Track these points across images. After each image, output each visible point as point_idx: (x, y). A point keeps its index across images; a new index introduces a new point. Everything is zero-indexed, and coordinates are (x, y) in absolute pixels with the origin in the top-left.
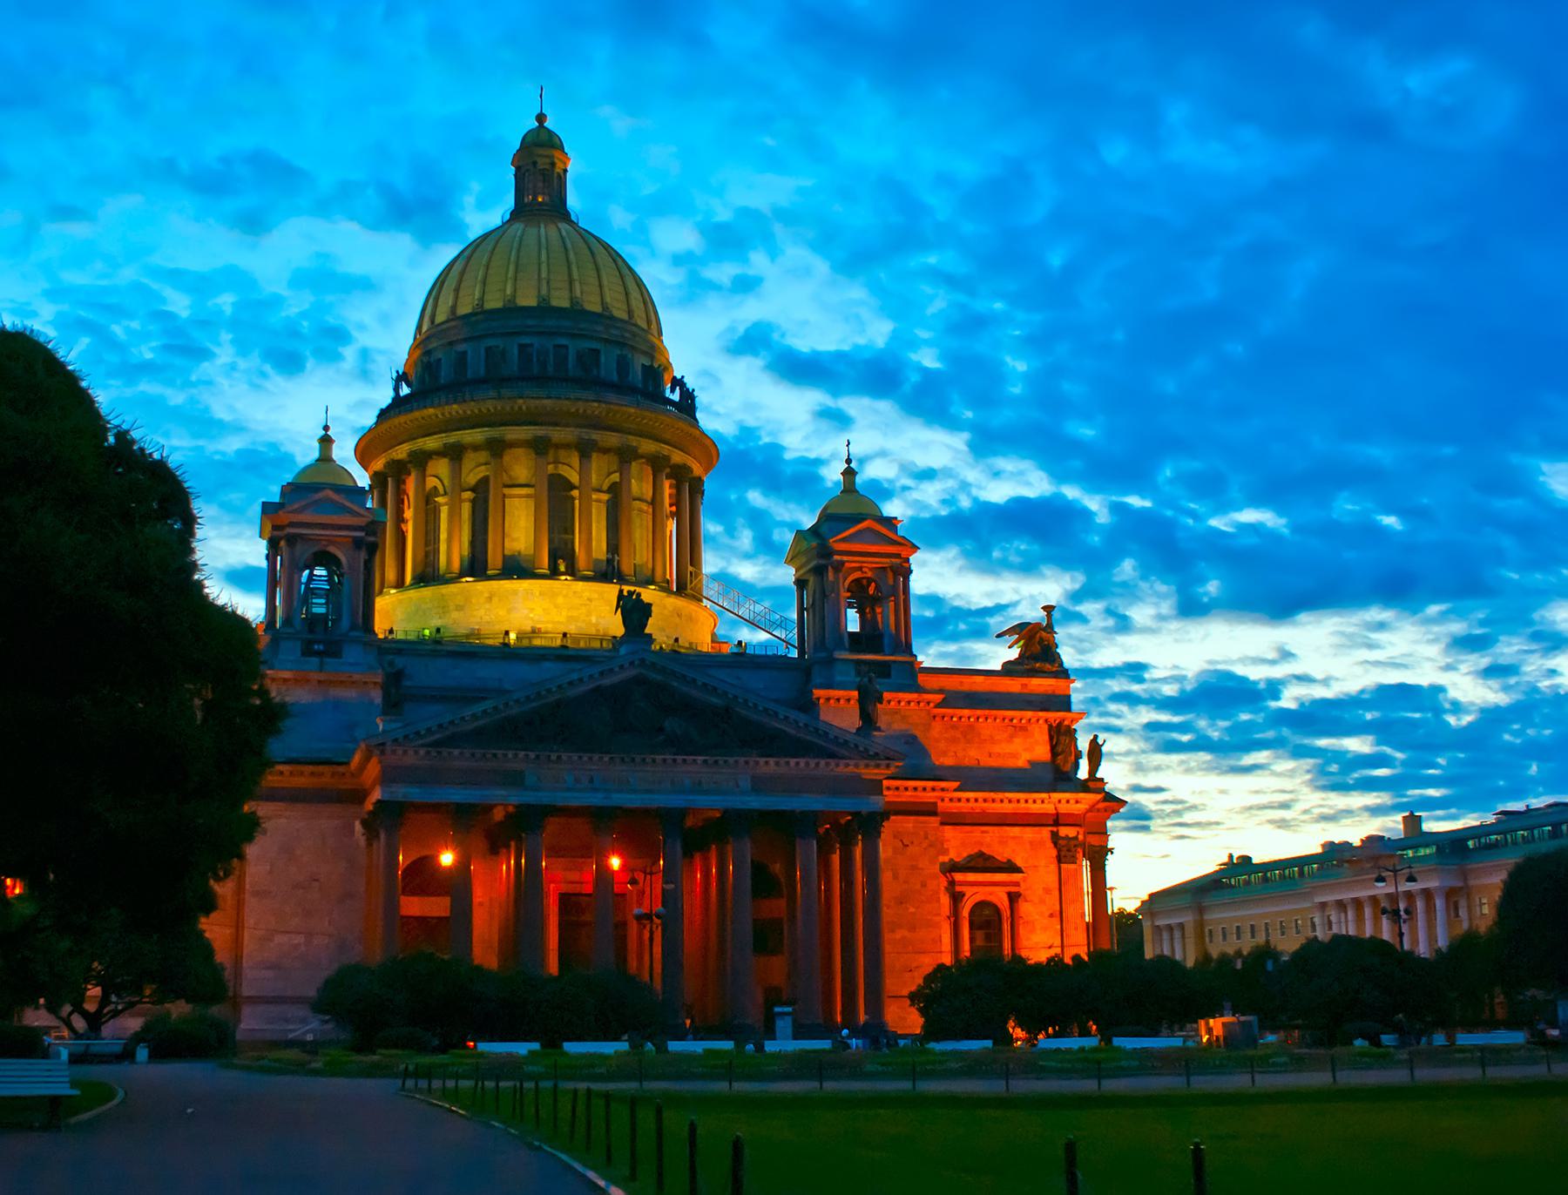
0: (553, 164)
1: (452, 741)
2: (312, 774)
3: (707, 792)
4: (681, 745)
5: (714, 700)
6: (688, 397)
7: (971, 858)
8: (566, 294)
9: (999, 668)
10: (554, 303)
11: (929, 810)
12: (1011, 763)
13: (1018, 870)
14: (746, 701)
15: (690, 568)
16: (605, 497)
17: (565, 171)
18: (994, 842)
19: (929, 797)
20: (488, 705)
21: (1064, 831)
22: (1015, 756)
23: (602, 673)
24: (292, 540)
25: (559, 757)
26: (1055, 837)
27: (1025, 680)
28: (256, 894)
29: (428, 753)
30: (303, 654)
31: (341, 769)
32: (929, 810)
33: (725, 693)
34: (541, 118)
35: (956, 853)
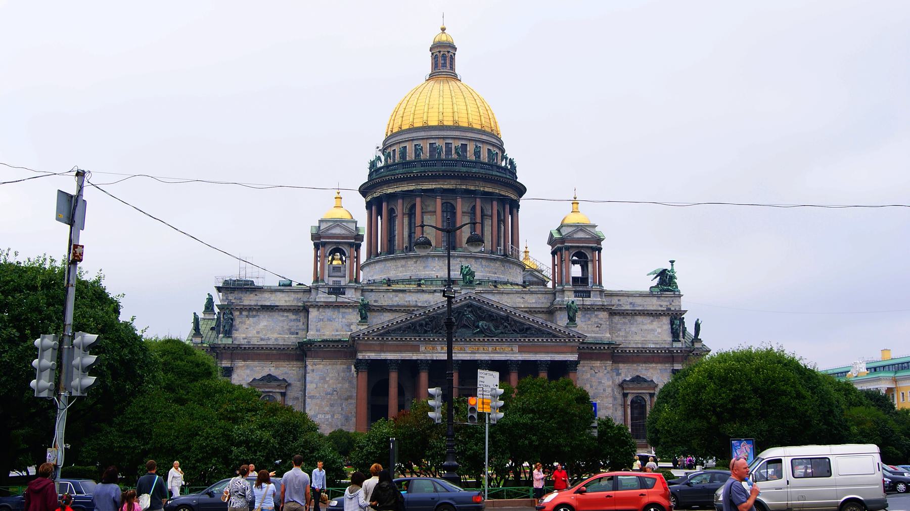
1: (388, 333)
3: (498, 353)
6: (511, 162)
8: (451, 119)
9: (648, 289)
10: (446, 123)
22: (653, 330)
24: (324, 244)
28: (312, 397)
34: (443, 29)
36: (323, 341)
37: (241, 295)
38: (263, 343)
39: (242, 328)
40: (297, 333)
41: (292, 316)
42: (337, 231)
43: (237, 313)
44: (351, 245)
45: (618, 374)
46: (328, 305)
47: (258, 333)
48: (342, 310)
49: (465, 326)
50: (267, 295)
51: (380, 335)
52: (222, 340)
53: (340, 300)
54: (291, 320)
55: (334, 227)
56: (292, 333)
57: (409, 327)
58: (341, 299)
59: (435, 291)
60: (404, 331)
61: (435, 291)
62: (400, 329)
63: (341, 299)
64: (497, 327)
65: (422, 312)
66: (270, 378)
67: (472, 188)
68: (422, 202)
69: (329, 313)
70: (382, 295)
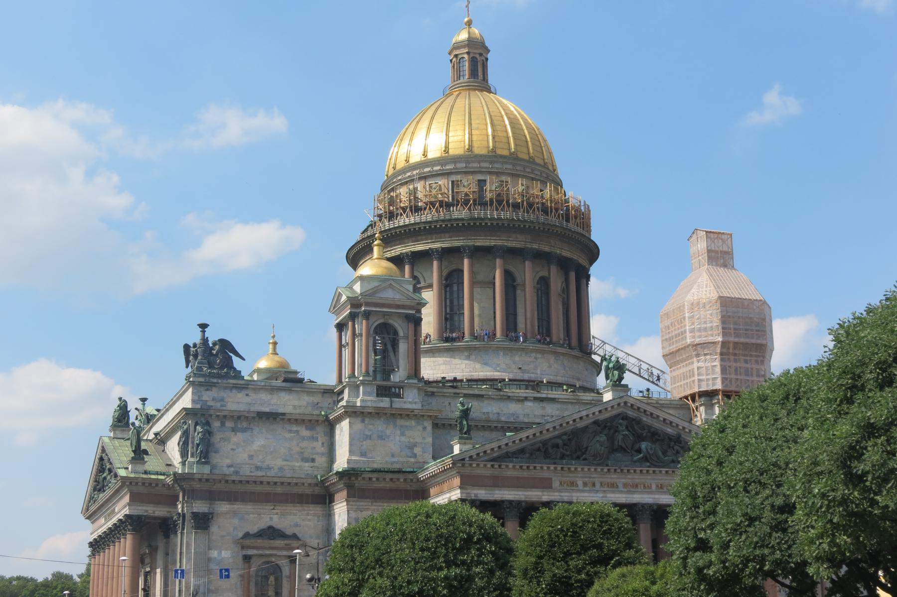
2: (391, 479)
4: (649, 460)
5: (669, 430)
10: (499, 152)
14: (690, 431)
17: (487, 59)
20: (530, 432)
23: (600, 412)
25: (576, 469)
29: (492, 466)
30: (378, 395)
31: (410, 476)
33: (677, 425)
36: (374, 471)
37: (223, 394)
38: (260, 473)
39: (225, 448)
40: (313, 460)
41: (305, 432)
42: (389, 295)
43: (216, 424)
44: (408, 318)
46: (378, 414)
47: (251, 457)
48: (400, 422)
49: (622, 449)
50: (264, 396)
51: (493, 460)
52: (194, 468)
53: (395, 405)
54: (303, 439)
55: (385, 289)
56: (305, 460)
57: (539, 450)
58: (398, 403)
59: (526, 399)
60: (531, 454)
61: (526, 399)
62: (522, 451)
63: (398, 403)
64: (665, 453)
65: (557, 424)
66: (271, 533)
67: (546, 249)
68: (471, 266)
69: (379, 426)
70: (446, 401)
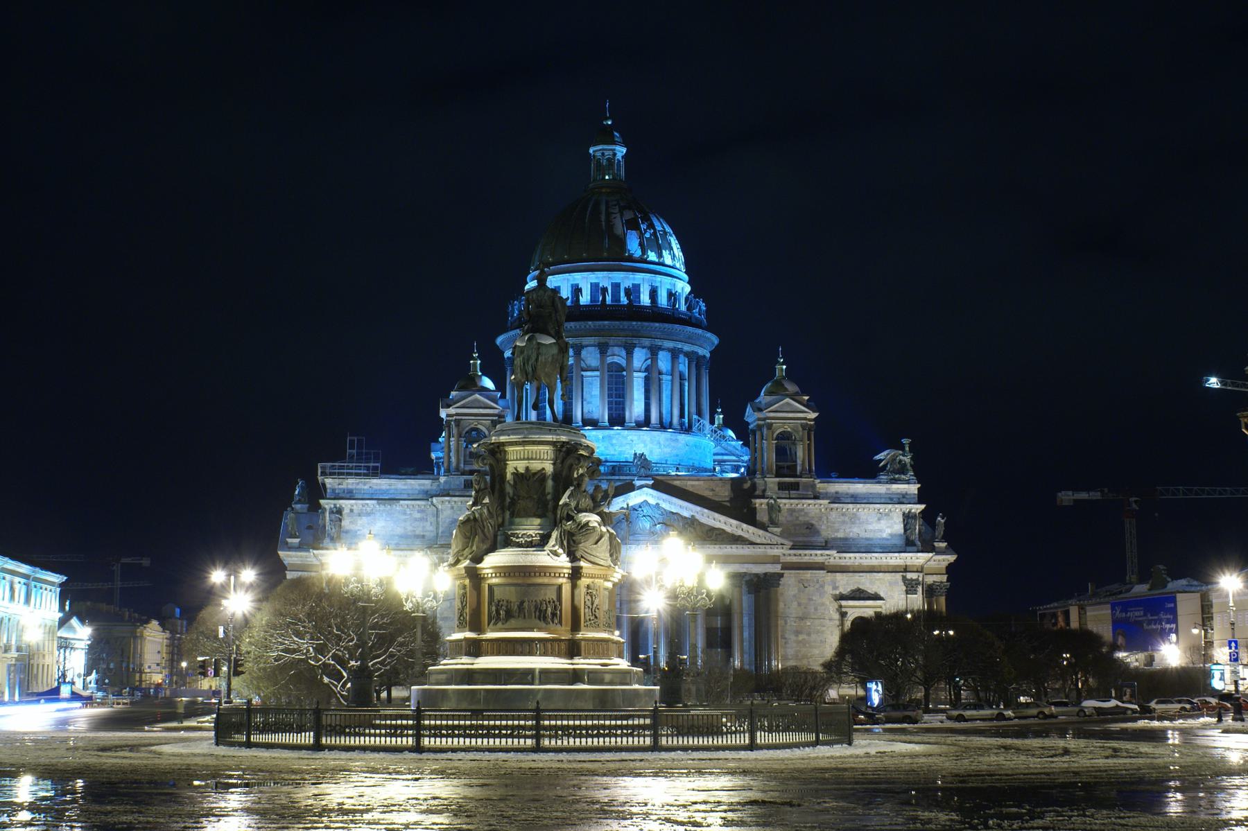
0: (615, 155)
7: (853, 591)
11: (821, 567)
12: (878, 535)
13: (881, 598)
15: (695, 417)
16: (643, 375)
18: (868, 583)
19: (819, 559)
21: (909, 576)
22: (881, 531)
26: (904, 578)
27: (888, 486)
32: (821, 567)
35: (845, 589)
45: (835, 588)
54: (416, 520)
